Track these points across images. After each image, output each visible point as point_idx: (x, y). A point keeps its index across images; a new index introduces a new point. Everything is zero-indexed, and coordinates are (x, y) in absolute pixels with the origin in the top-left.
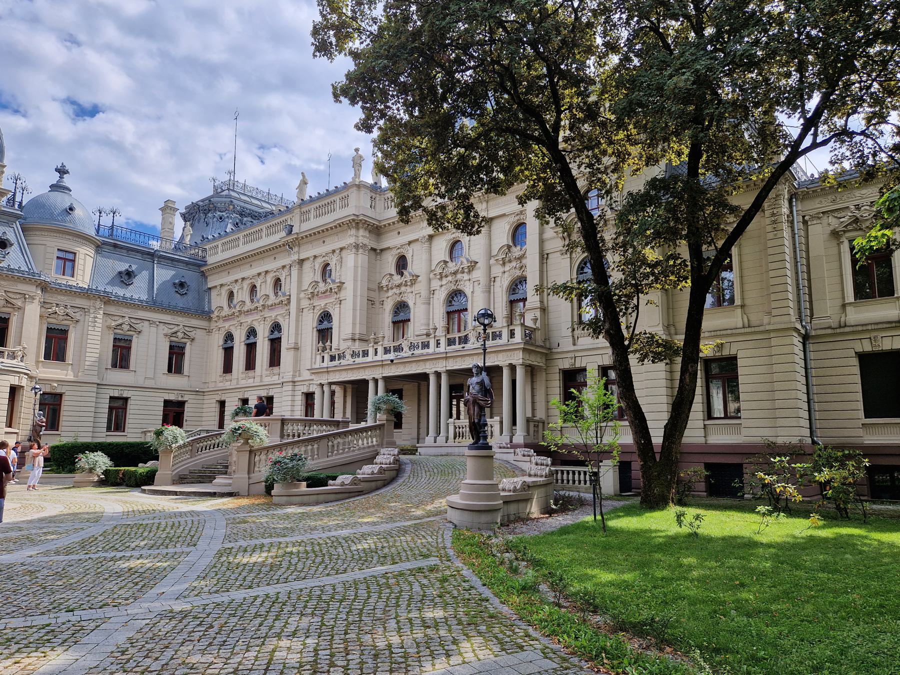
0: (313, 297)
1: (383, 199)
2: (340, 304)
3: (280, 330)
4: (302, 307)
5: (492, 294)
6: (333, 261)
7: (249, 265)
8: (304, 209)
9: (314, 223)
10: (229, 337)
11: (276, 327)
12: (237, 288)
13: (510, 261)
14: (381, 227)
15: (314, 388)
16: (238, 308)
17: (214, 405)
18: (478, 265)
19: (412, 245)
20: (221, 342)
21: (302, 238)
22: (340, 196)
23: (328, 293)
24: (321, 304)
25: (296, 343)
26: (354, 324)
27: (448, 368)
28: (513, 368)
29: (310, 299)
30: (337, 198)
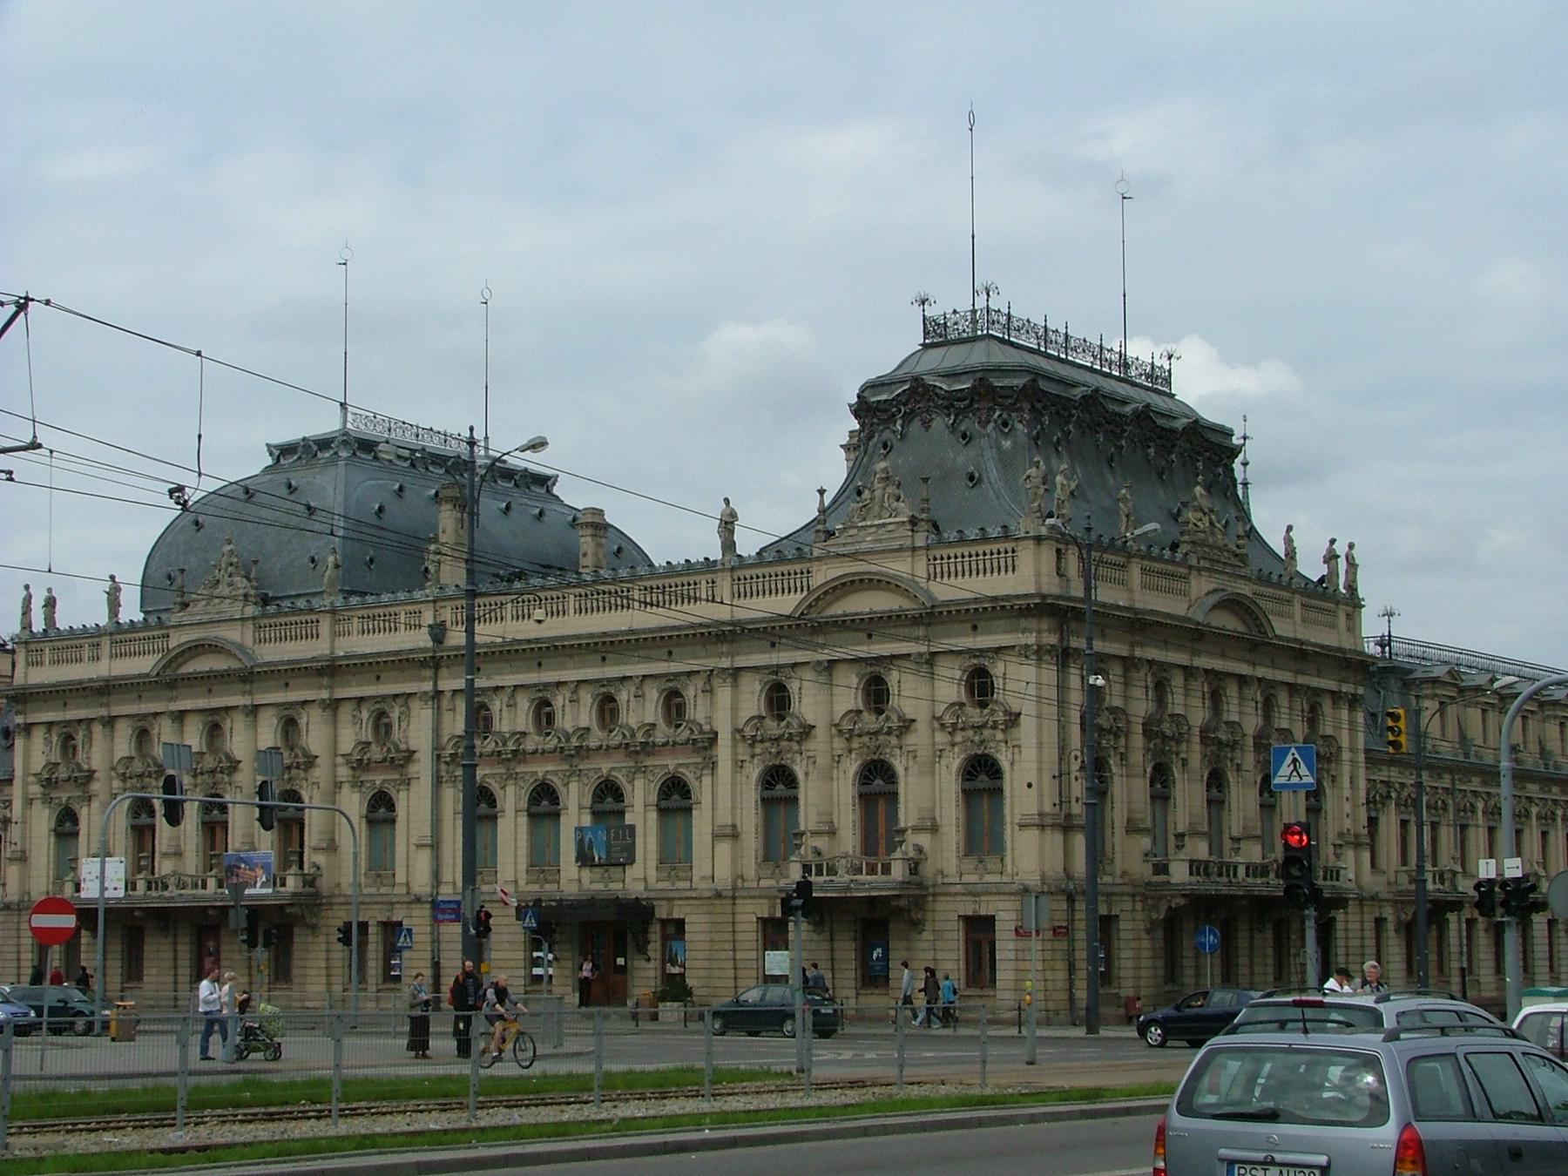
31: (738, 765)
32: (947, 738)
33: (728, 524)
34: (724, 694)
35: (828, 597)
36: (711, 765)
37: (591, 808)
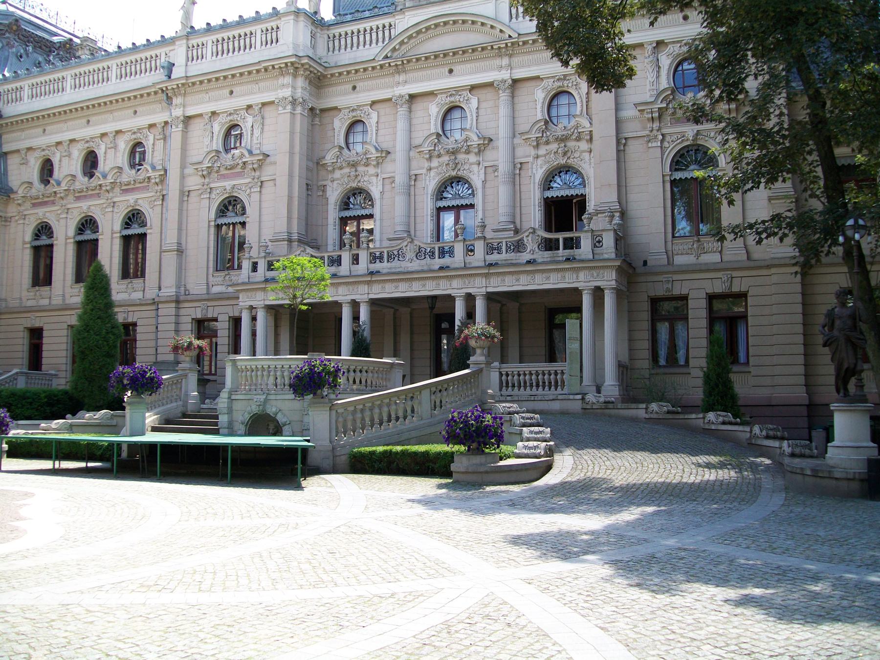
0: (209, 173)
1: (326, 37)
2: (261, 187)
3: (143, 224)
4: (187, 189)
5: (517, 187)
6: (247, 123)
7: (84, 121)
8: (194, 42)
9: (209, 64)
10: (44, 230)
11: (134, 217)
12: (58, 155)
13: (547, 143)
14: (325, 76)
15: (222, 314)
16: (64, 186)
17: (21, 335)
18: (494, 144)
19: (376, 107)
20: (28, 237)
21: (194, 84)
22: (264, 26)
23: (238, 170)
24: (224, 187)
25: (179, 244)
26: (289, 218)
27: (490, 290)
28: (598, 293)
29: (204, 176)
30: (257, 28)
32: (533, 152)
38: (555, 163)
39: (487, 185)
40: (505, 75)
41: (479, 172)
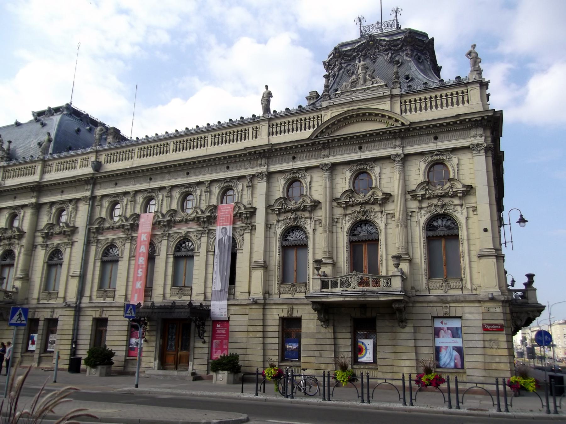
31: (268, 226)
33: (267, 97)
34: (261, 186)
35: (334, 127)
36: (250, 227)
37: (174, 254)
38: (436, 213)
39: (388, 227)
40: (399, 151)
41: (382, 217)
